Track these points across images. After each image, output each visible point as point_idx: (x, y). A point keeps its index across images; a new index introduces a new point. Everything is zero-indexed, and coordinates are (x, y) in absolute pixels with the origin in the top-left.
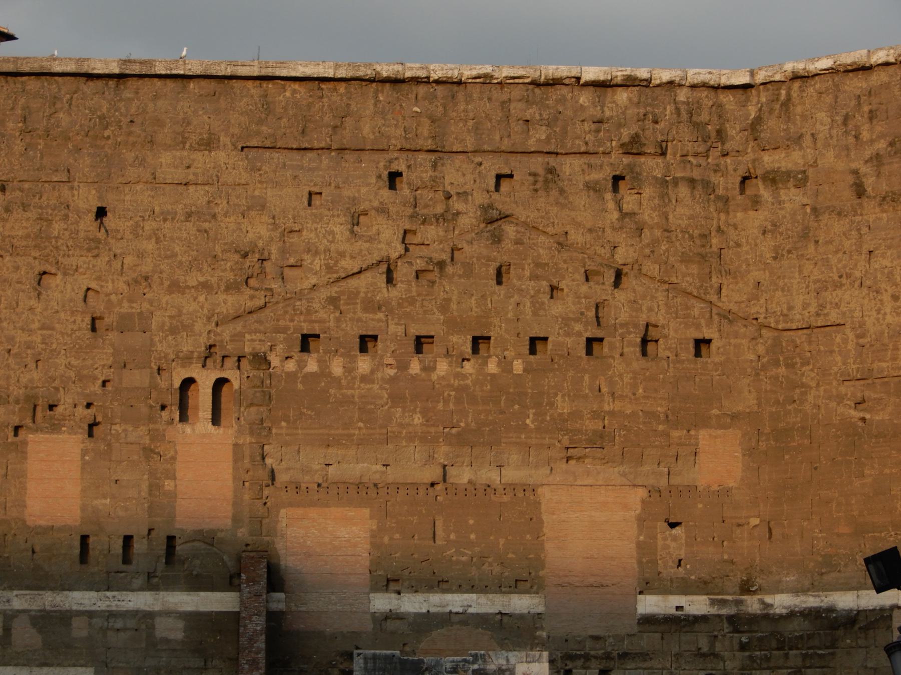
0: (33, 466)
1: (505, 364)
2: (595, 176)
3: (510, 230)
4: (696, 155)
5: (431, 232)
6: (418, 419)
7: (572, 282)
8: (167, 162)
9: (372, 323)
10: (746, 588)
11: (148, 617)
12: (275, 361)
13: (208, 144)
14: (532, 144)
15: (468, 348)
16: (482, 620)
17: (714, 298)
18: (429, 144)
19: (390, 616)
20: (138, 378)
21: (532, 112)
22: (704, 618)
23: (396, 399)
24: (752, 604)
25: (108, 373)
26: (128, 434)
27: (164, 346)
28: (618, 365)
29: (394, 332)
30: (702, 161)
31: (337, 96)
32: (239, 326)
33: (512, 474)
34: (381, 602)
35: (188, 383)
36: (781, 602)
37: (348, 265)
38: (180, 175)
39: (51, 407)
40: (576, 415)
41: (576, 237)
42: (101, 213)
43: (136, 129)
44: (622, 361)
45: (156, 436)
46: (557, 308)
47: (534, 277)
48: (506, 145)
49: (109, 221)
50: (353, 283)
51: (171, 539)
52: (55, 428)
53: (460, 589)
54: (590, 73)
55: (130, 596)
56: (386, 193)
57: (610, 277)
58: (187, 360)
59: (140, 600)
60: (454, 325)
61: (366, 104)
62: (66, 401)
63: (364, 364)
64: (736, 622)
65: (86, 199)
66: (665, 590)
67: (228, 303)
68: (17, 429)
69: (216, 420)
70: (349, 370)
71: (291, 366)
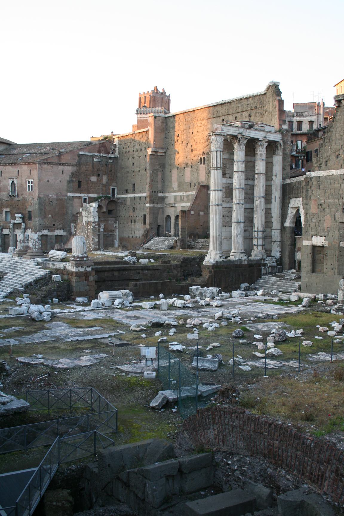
0: (186, 173)
13: (203, 120)
21: (240, 105)
45: (197, 167)
61: (219, 108)
65: (191, 131)
69: (204, 163)
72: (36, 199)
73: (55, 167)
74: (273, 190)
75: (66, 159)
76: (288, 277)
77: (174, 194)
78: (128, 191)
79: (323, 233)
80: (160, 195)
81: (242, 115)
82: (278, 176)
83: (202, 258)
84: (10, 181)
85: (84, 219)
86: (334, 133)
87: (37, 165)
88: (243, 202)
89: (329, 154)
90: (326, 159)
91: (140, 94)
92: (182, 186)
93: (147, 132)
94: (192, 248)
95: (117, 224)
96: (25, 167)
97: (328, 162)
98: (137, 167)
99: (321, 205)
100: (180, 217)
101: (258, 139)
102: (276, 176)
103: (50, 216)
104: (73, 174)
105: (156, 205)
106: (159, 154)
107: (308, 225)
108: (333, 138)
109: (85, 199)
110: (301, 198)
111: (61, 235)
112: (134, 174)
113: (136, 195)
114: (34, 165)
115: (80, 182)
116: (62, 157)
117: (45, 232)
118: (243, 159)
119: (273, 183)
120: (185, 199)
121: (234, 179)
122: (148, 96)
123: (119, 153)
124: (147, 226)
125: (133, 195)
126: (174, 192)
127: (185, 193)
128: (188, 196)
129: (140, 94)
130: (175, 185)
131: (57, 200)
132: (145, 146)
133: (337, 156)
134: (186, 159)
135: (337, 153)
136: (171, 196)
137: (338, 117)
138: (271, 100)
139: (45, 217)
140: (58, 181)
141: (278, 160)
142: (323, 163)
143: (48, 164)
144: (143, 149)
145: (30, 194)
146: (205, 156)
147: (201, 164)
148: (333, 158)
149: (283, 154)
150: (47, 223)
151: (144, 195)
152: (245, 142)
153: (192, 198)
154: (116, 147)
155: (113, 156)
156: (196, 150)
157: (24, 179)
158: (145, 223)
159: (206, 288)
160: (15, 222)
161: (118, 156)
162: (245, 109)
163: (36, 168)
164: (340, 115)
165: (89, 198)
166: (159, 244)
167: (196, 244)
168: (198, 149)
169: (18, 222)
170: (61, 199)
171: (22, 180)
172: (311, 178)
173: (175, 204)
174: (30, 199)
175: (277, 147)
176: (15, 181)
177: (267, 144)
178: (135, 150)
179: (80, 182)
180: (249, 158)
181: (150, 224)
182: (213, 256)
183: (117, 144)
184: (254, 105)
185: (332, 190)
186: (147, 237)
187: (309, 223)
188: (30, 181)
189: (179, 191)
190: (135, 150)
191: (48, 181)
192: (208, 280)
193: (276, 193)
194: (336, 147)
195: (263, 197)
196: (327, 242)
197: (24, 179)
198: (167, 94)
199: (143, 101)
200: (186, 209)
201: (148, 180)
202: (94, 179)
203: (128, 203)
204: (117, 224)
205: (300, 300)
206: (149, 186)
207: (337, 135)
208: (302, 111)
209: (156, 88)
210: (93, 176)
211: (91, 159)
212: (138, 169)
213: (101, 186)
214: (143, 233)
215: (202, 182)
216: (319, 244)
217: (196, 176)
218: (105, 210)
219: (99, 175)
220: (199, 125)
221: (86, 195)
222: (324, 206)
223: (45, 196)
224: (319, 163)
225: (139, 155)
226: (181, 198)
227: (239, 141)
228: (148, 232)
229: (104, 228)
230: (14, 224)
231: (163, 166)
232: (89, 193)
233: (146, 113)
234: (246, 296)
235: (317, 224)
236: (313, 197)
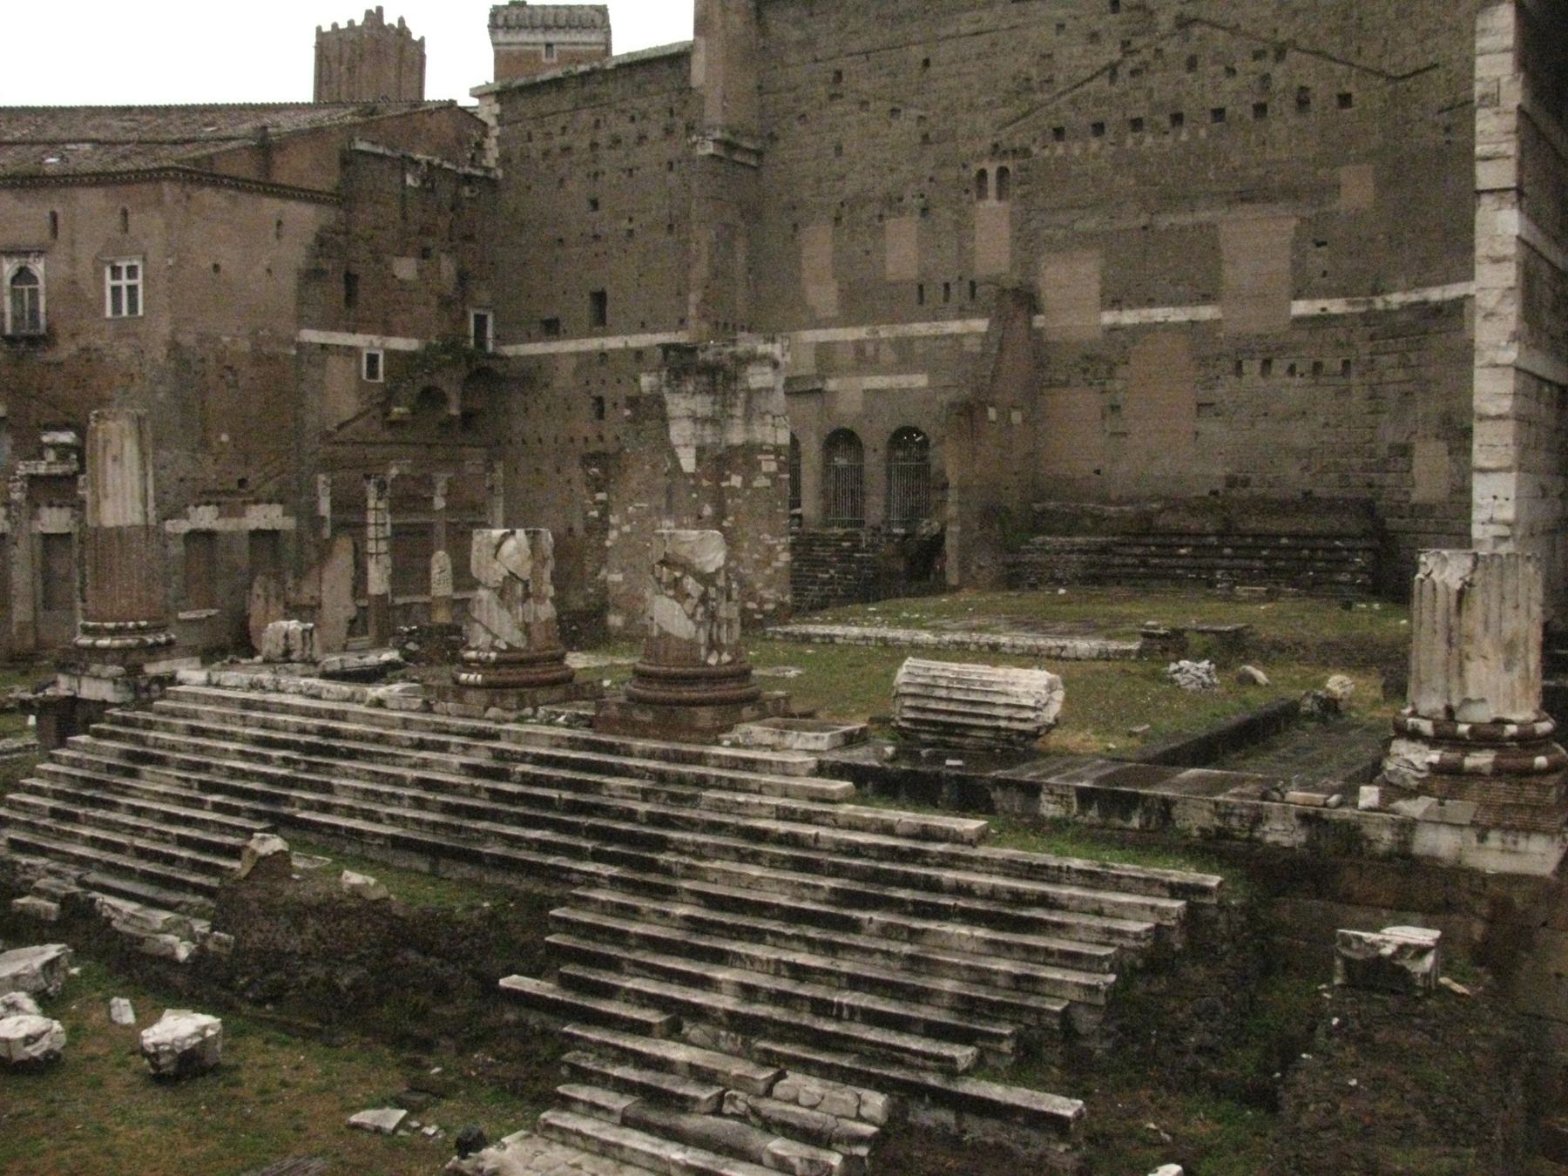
1: (1194, 135)
3: (1196, 31)
5: (1138, 43)
6: (1132, 182)
7: (1246, 65)
9: (1100, 114)
10: (1376, 291)
11: (956, 338)
12: (1035, 150)
15: (1166, 123)
16: (1178, 325)
17: (1352, 58)
19: (1114, 328)
20: (952, 173)
22: (1343, 316)
23: (1117, 167)
24: (1379, 304)
26: (945, 215)
28: (1276, 125)
29: (1114, 118)
32: (1010, 129)
33: (1204, 216)
34: (1108, 318)
36: (1396, 299)
37: (1087, 73)
38: (973, 27)
39: (900, 200)
40: (1244, 167)
41: (1246, 26)
42: (926, 63)
44: (1283, 121)
46: (1229, 85)
47: (1214, 62)
49: (934, 70)
50: (1087, 87)
52: (901, 213)
53: (1163, 304)
55: (949, 324)
56: (1111, 17)
57: (1271, 53)
58: (979, 157)
59: (955, 327)
60: (1158, 107)
63: (1095, 144)
64: (1368, 318)
65: (917, 53)
66: (1312, 295)
67: (1006, 112)
68: (881, 217)
69: (1000, 197)
70: (1085, 150)
71: (1047, 153)
72: (160, 353)
73: (246, 199)
75: (293, 167)
77: (810, 336)
78: (564, 325)
84: (9, 268)
85: (680, 432)
87: (166, 187)
91: (319, 29)
92: (860, 300)
95: (500, 474)
96: (92, 200)
98: (618, 216)
103: (224, 438)
104: (321, 241)
106: (738, 157)
109: (373, 359)
111: (274, 534)
112: (598, 247)
113: (614, 343)
114: (145, 187)
115: (350, 280)
116: (278, 158)
117: (205, 518)
120: (888, 356)
123: (505, 160)
125: (593, 344)
126: (818, 324)
128: (903, 346)
129: (319, 29)
130: (823, 296)
131: (258, 359)
132: (664, 120)
139: (205, 444)
140: (260, 270)
143: (216, 181)
144: (655, 133)
145: (123, 329)
146: (1010, 164)
147: (982, 195)
150: (210, 472)
154: (485, 135)
155: (479, 173)
157: (86, 254)
160: (42, 469)
161: (500, 173)
163: (159, 202)
165: (391, 354)
168: (962, 130)
169: (58, 470)
170: (272, 359)
171: (73, 261)
173: (823, 379)
174: (124, 353)
176: (38, 268)
178: (603, 137)
179: (350, 280)
183: (492, 122)
188: (124, 264)
190: (603, 137)
191: (216, 268)
197: (86, 254)
198: (416, 37)
201: (701, 270)
202: (406, 268)
203: (564, 379)
204: (500, 474)
209: (375, 17)
210: (404, 255)
211: (397, 180)
212: (625, 223)
213: (434, 301)
215: (992, 281)
218: (455, 411)
219: (425, 254)
220: (966, 28)
221: (376, 340)
223: (202, 339)
229: (447, 496)
230: (33, 479)
231: (753, 213)
232: (389, 332)
233: (534, 27)
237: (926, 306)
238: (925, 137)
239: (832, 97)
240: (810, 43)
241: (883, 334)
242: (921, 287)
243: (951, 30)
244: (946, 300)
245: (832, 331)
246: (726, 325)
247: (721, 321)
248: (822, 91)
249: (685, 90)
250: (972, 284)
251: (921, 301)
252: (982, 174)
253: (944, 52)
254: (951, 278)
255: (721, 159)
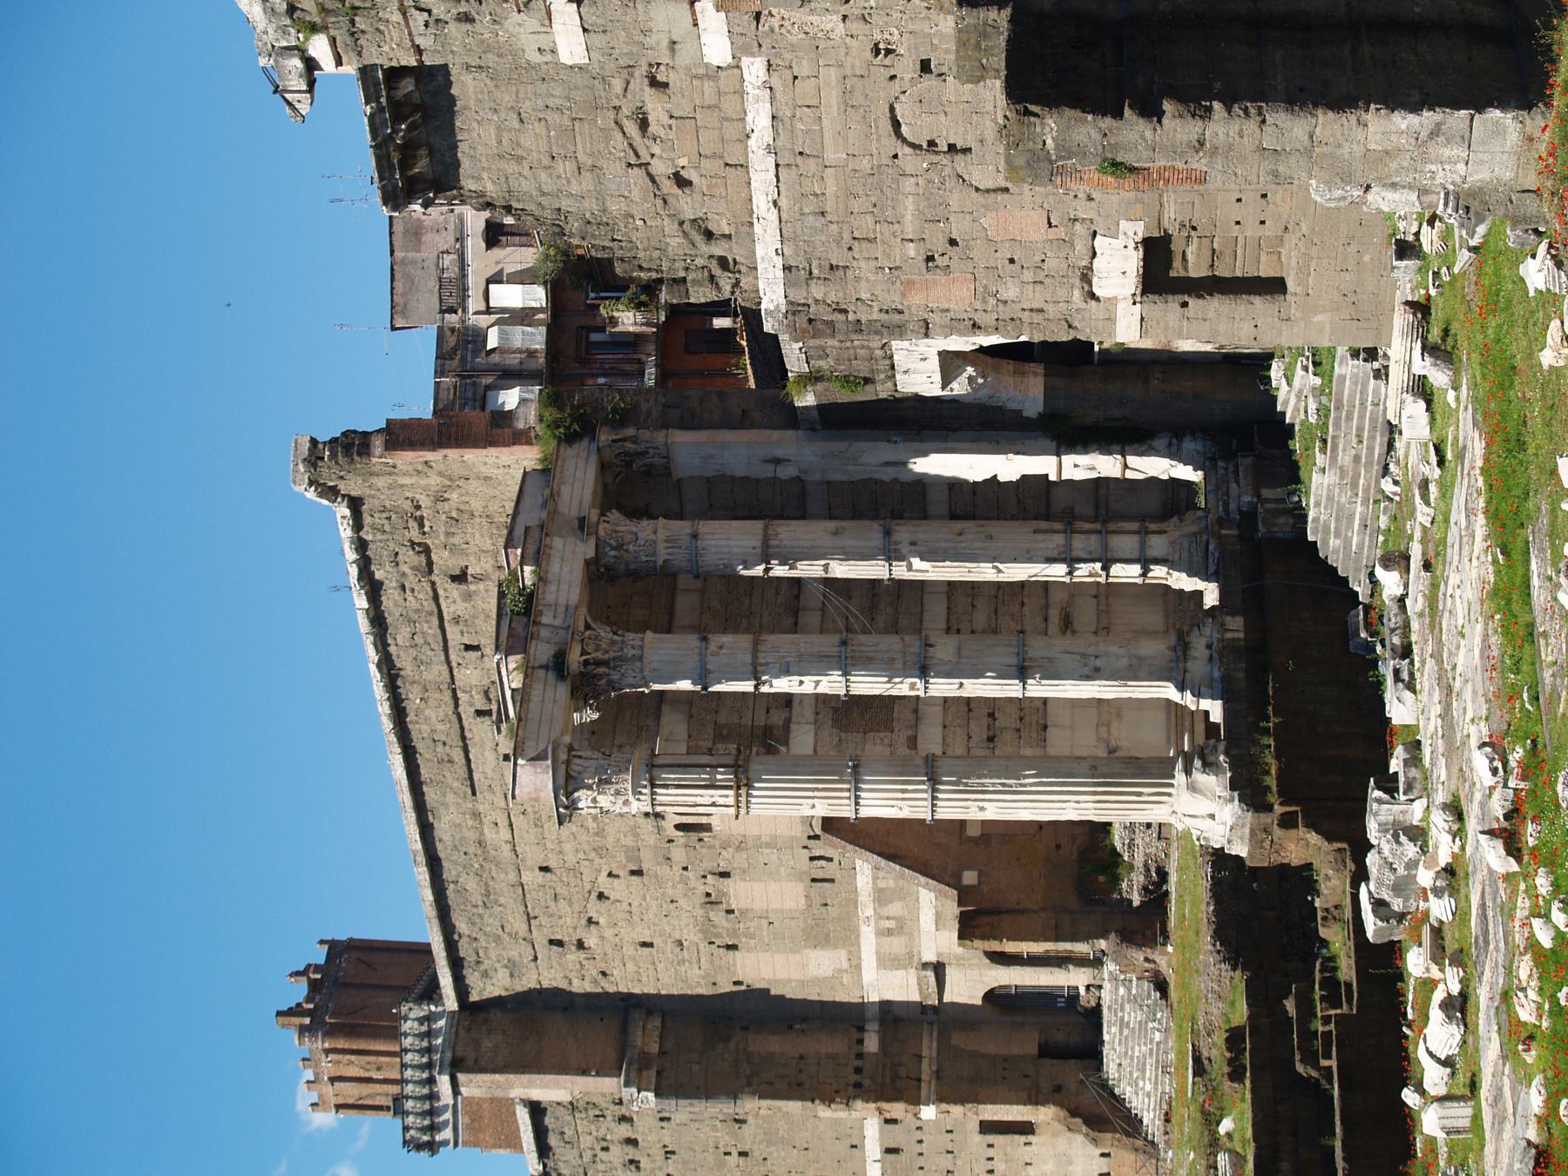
0: (758, 905)
2: (456, 594)
4: (421, 525)
8: (497, 837)
13: (476, 815)
14: (432, 629)
18: (448, 695)
20: (678, 854)
25: (677, 869)
27: (652, 840)
30: (427, 523)
31: (420, 746)
35: (678, 827)
39: (708, 895)
42: (545, 869)
43: (471, 850)
48: (438, 647)
49: (552, 864)
51: (810, 838)
52: (725, 894)
54: (362, 602)
62: (701, 889)
65: (531, 877)
74: (855, 473)
76: (1312, 406)
79: (1081, 247)
80: (872, 1044)
81: (456, 620)
82: (778, 452)
83: (1219, 859)
86: (565, 204)
88: (914, 643)
89: (670, 227)
90: (699, 239)
92: (828, 925)
93: (537, 1110)
94: (1163, 875)
97: (712, 227)
99: (930, 259)
100: (995, 946)
101: (587, 563)
102: (777, 461)
105: (926, 1070)
106: (654, 1048)
107: (1037, 318)
108: (591, 206)
110: (895, 344)
118: (692, 640)
119: (817, 477)
120: (895, 909)
121: (795, 689)
122: (328, 1066)
124: (1043, 1115)
126: (858, 967)
127: (867, 909)
128: (881, 897)
132: (609, 1121)
133: (682, 182)
134: (682, 902)
135: (668, 187)
136: (886, 983)
137: (491, 189)
138: (381, 482)
141: (691, 451)
142: (718, 249)
144: (624, 1131)
148: (687, 206)
149: (666, 425)
151: (872, 1129)
152: (605, 633)
153: (893, 873)
156: (633, 853)
158: (1026, 1128)
159: (1371, 859)
162: (429, 605)
164: (479, 179)
166: (1141, 1058)
167: (1139, 861)
168: (629, 841)
172: (794, 309)
175: (628, 459)
177: (614, 515)
180: (685, 604)
181: (1035, 1099)
182: (1202, 805)
184: (410, 558)
185: (856, 205)
186: (1105, 1115)
187: (1026, 316)
189: (850, 939)
192: (1330, 838)
193: (865, 459)
194: (636, 195)
195: (888, 533)
196: (1124, 225)
198: (319, 956)
199: (352, 1092)
200: (952, 909)
201: (794, 1107)
205: (1421, 389)
206: (828, 1100)
207: (575, 188)
208: (433, 284)
214: (1079, 1138)
216: (1133, 261)
217: (770, 855)
220: (505, 834)
222: (938, 244)
224: (717, 271)
225: (659, 1154)
226: (889, 932)
227: (599, 663)
228: (1074, 1113)
234: (1406, 652)
235: (1028, 276)
236: (893, 299)
237: (838, 876)
238: (633, 873)
239: (580, 945)
240: (513, 968)
241: (870, 912)
242: (813, 880)
243: (508, 847)
244: (830, 860)
245: (863, 955)
246: (858, 1071)
247: (854, 1078)
248: (573, 956)
249: (573, 1106)
250: (810, 838)
251: (832, 881)
252: (678, 827)
253: (532, 855)
254: (806, 854)
255: (658, 1073)
